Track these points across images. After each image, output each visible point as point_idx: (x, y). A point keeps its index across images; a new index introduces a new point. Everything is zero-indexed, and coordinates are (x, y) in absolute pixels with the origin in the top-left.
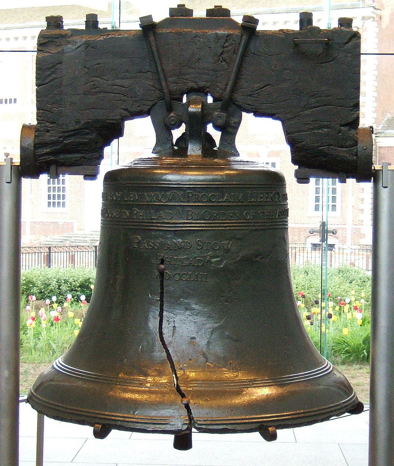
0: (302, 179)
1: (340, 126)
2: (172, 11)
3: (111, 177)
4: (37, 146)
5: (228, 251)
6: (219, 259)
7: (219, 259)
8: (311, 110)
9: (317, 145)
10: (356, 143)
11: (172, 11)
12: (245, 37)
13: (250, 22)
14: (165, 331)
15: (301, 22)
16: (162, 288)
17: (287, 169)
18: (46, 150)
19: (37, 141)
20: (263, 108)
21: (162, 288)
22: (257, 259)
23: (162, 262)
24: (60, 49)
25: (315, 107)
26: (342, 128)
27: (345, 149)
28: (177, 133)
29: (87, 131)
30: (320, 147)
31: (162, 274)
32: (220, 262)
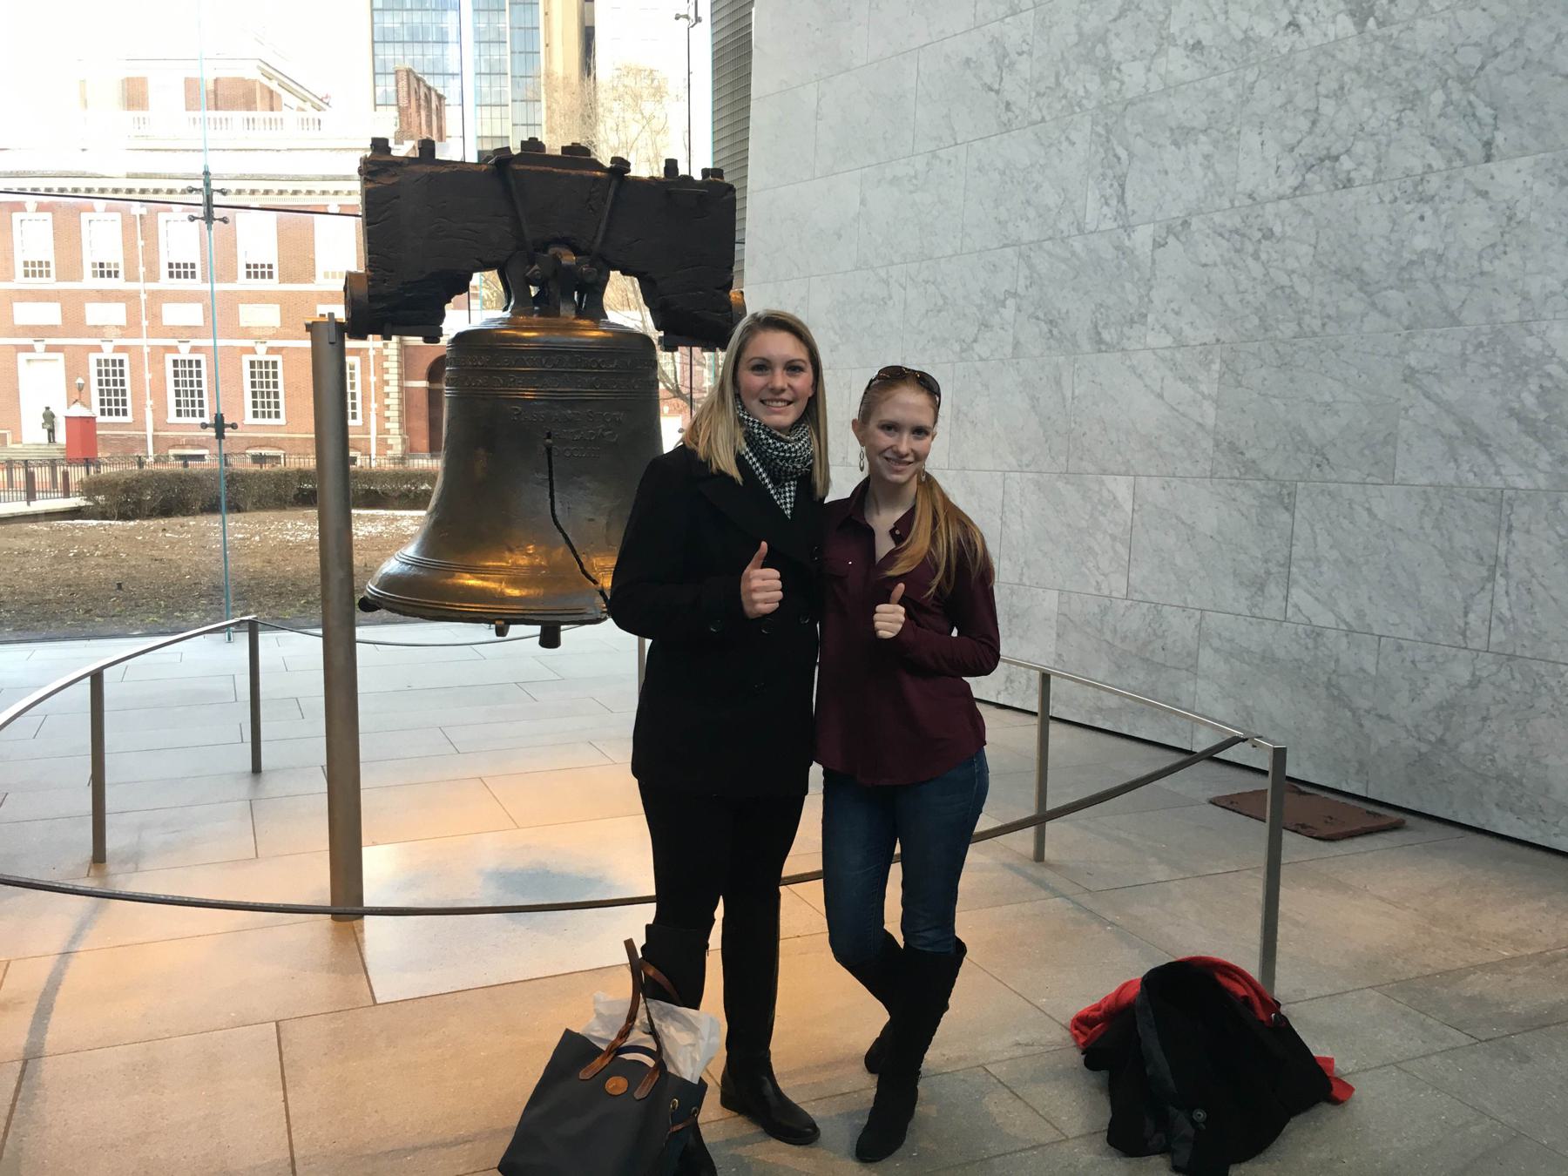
0: (670, 347)
2: (523, 143)
3: (461, 339)
4: (372, 298)
11: (523, 143)
12: (615, 182)
13: (621, 165)
14: (557, 512)
15: (666, 169)
16: (550, 467)
17: (655, 335)
21: (550, 467)
23: (549, 436)
24: (395, 180)
28: (534, 291)
31: (549, 450)
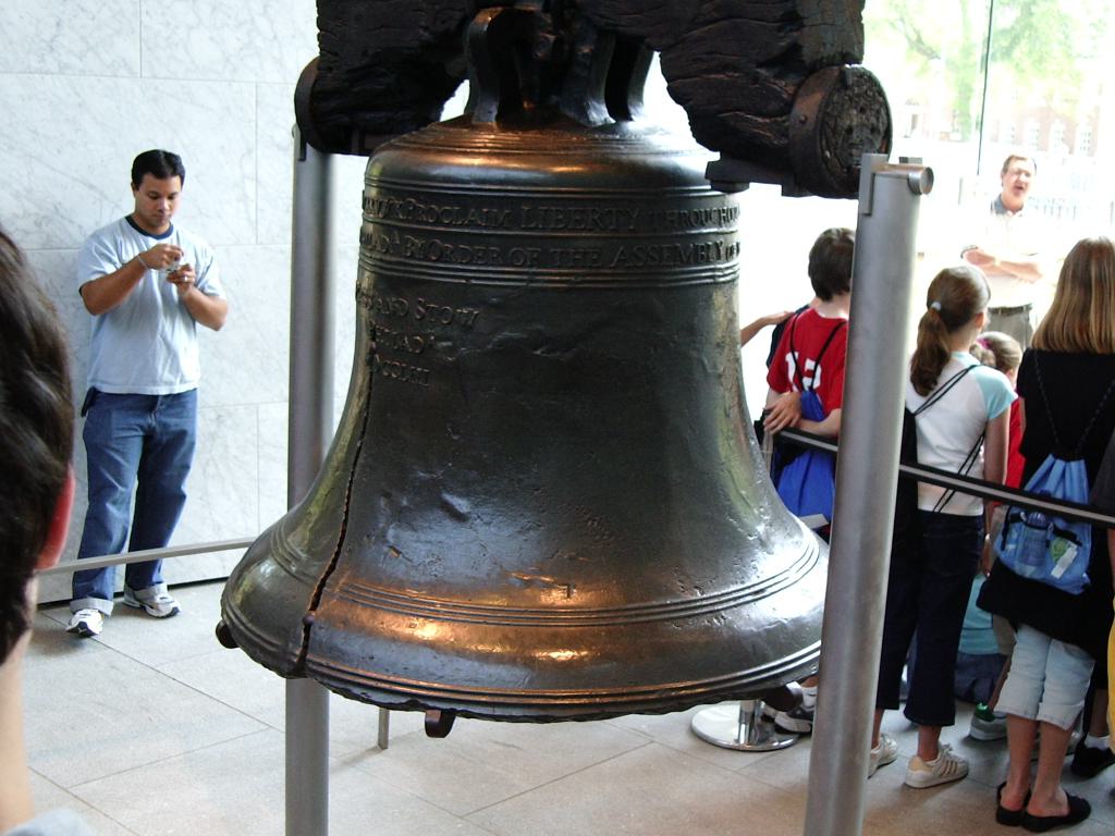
1: (760, 65)
5: (467, 329)
6: (450, 344)
7: (450, 344)
8: (706, 28)
9: (716, 107)
10: (788, 107)
18: (333, 104)
19: (318, 88)
20: (623, 23)
22: (538, 352)
25: (711, 22)
26: (762, 71)
27: (768, 121)
29: (383, 70)
30: (722, 113)
32: (451, 351)
